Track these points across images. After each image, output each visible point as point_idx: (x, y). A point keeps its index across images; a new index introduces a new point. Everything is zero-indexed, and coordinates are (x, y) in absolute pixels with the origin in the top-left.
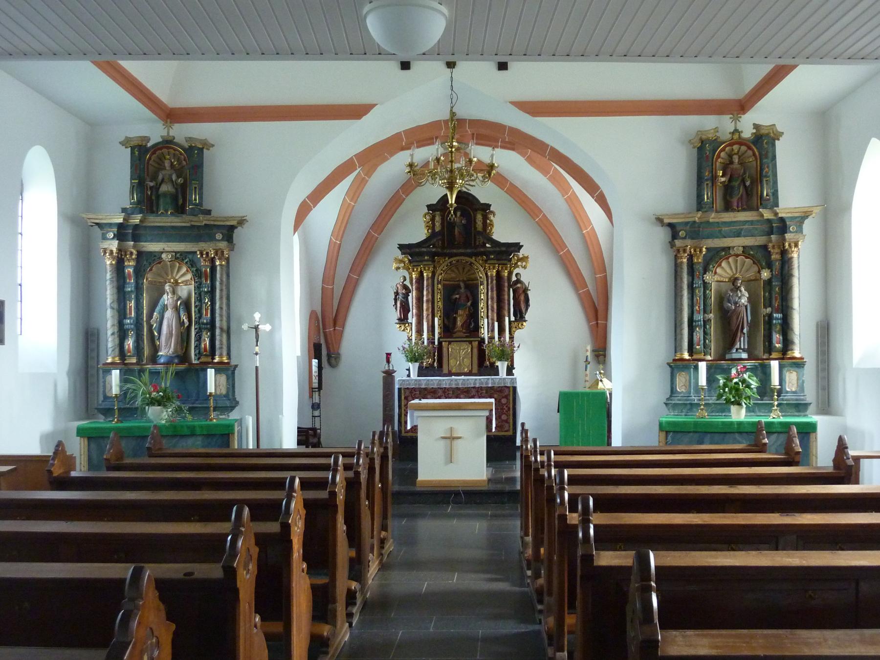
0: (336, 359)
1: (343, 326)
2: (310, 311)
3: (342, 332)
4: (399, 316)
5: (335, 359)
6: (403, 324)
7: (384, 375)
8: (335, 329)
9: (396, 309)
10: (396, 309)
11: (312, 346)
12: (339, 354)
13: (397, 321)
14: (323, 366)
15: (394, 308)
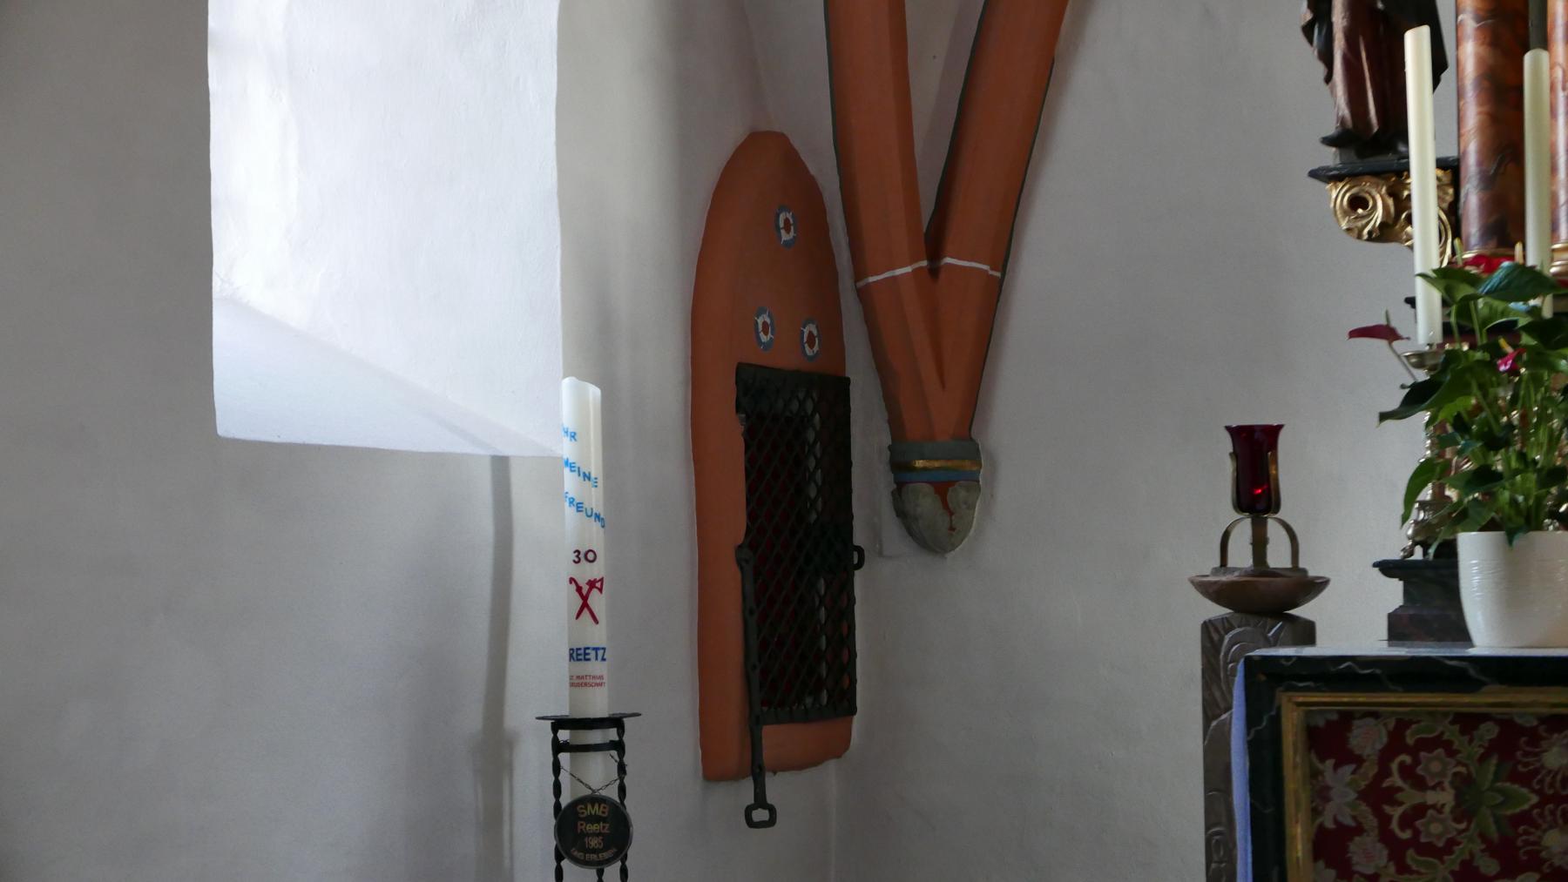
0: (942, 489)
1: (1003, 251)
2: (732, 135)
3: (993, 294)
4: (1345, 111)
5: (942, 489)
6: (1378, 174)
7: (1218, 611)
8: (934, 271)
9: (1326, 57)
10: (1327, 58)
11: (725, 390)
12: (974, 454)
13: (1330, 157)
14: (858, 539)
15: (1310, 53)
